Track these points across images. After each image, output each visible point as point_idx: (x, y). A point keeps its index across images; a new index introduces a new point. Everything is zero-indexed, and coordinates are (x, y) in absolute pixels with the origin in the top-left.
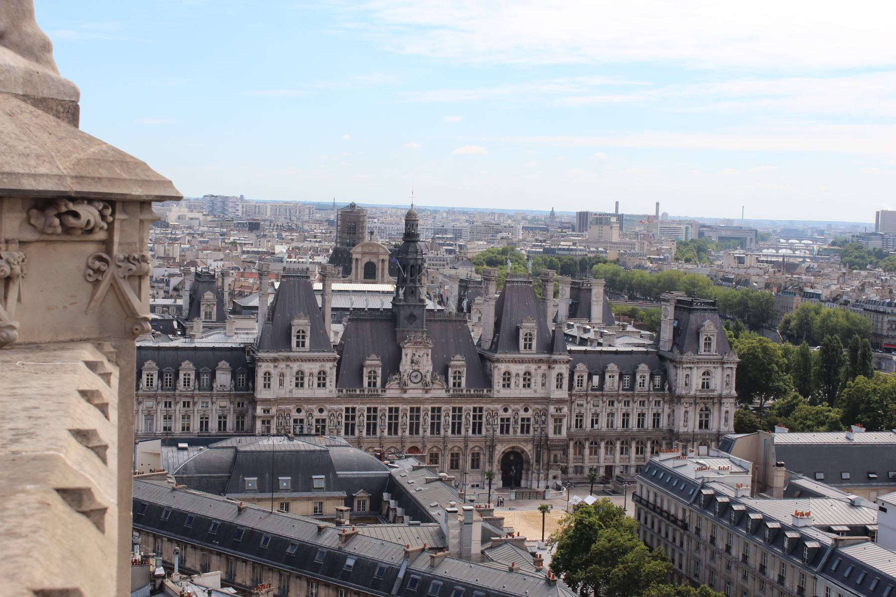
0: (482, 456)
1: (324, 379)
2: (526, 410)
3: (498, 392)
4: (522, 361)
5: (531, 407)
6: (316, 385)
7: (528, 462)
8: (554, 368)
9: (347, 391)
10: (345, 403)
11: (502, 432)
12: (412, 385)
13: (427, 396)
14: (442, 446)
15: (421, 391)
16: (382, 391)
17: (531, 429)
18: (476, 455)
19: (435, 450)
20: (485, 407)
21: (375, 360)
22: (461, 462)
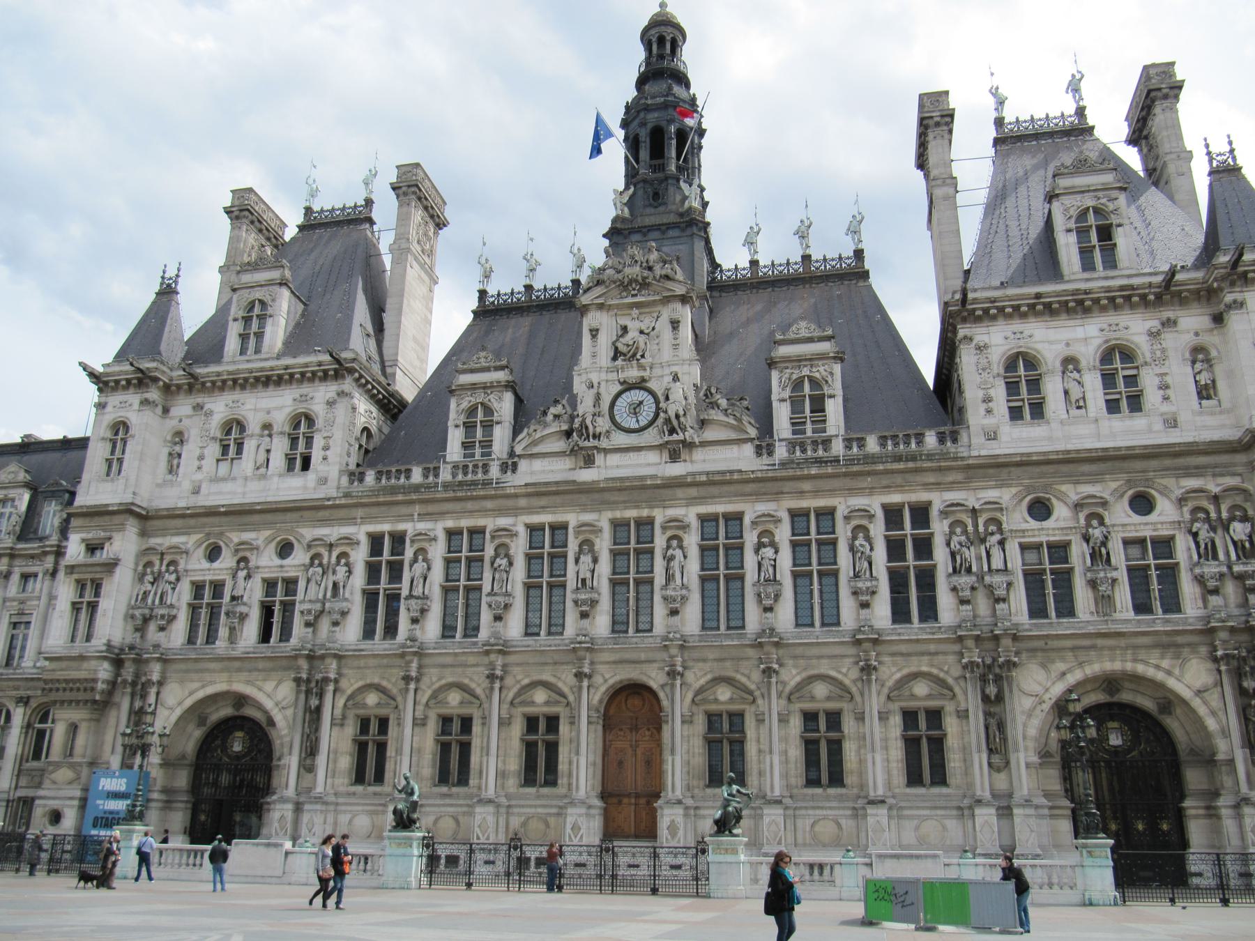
0: (951, 725)
1: (309, 441)
2: (1142, 504)
3: (992, 436)
4: (1079, 306)
5: (1165, 492)
6: (278, 461)
7: (1208, 760)
8: (1240, 305)
9: (378, 479)
10: (365, 520)
11: (1037, 610)
12: (620, 439)
13: (677, 469)
14: (756, 676)
15: (653, 457)
16: (504, 468)
17: (1188, 589)
18: (923, 724)
19: (724, 694)
20: (938, 500)
21: (487, 369)
22: (850, 751)
